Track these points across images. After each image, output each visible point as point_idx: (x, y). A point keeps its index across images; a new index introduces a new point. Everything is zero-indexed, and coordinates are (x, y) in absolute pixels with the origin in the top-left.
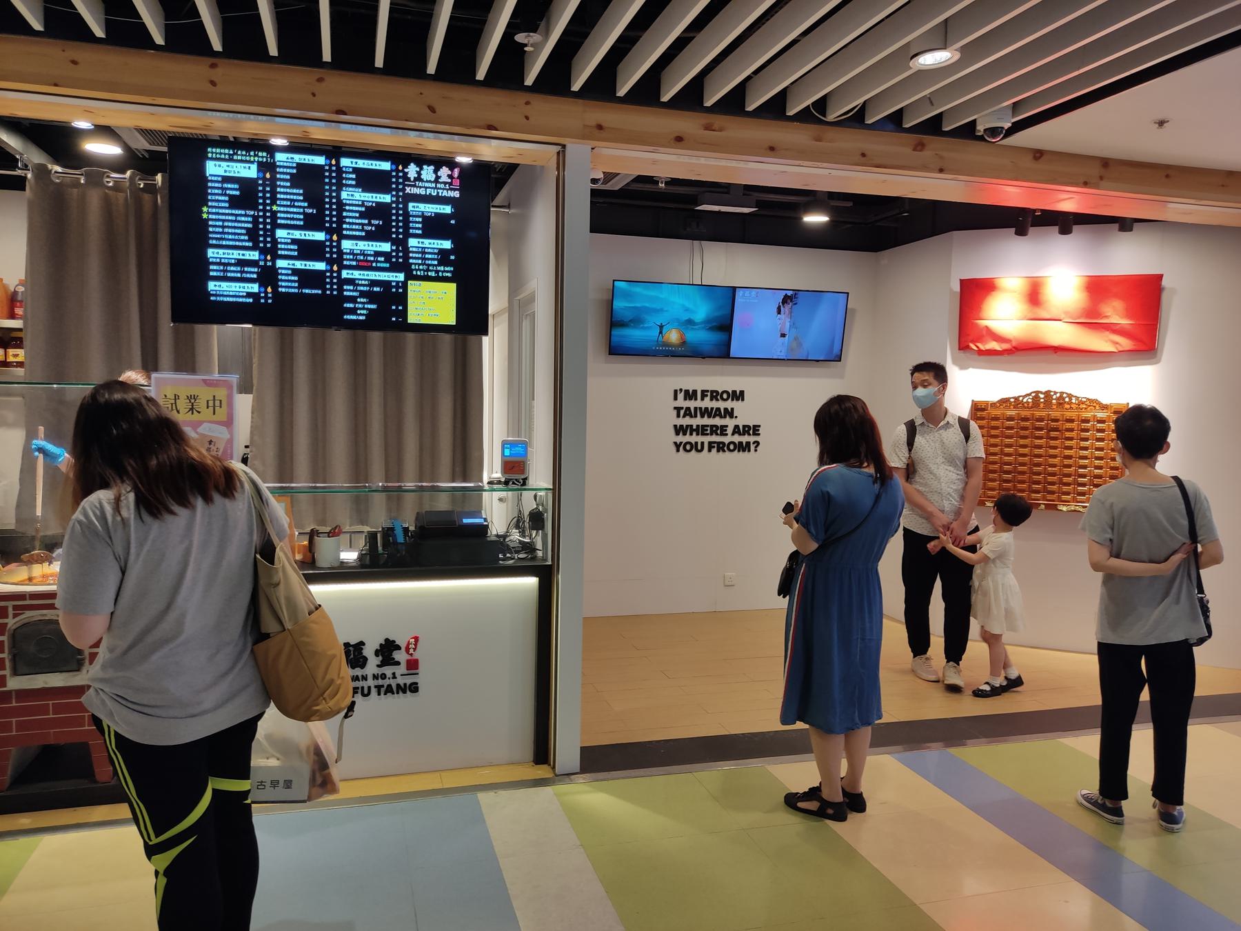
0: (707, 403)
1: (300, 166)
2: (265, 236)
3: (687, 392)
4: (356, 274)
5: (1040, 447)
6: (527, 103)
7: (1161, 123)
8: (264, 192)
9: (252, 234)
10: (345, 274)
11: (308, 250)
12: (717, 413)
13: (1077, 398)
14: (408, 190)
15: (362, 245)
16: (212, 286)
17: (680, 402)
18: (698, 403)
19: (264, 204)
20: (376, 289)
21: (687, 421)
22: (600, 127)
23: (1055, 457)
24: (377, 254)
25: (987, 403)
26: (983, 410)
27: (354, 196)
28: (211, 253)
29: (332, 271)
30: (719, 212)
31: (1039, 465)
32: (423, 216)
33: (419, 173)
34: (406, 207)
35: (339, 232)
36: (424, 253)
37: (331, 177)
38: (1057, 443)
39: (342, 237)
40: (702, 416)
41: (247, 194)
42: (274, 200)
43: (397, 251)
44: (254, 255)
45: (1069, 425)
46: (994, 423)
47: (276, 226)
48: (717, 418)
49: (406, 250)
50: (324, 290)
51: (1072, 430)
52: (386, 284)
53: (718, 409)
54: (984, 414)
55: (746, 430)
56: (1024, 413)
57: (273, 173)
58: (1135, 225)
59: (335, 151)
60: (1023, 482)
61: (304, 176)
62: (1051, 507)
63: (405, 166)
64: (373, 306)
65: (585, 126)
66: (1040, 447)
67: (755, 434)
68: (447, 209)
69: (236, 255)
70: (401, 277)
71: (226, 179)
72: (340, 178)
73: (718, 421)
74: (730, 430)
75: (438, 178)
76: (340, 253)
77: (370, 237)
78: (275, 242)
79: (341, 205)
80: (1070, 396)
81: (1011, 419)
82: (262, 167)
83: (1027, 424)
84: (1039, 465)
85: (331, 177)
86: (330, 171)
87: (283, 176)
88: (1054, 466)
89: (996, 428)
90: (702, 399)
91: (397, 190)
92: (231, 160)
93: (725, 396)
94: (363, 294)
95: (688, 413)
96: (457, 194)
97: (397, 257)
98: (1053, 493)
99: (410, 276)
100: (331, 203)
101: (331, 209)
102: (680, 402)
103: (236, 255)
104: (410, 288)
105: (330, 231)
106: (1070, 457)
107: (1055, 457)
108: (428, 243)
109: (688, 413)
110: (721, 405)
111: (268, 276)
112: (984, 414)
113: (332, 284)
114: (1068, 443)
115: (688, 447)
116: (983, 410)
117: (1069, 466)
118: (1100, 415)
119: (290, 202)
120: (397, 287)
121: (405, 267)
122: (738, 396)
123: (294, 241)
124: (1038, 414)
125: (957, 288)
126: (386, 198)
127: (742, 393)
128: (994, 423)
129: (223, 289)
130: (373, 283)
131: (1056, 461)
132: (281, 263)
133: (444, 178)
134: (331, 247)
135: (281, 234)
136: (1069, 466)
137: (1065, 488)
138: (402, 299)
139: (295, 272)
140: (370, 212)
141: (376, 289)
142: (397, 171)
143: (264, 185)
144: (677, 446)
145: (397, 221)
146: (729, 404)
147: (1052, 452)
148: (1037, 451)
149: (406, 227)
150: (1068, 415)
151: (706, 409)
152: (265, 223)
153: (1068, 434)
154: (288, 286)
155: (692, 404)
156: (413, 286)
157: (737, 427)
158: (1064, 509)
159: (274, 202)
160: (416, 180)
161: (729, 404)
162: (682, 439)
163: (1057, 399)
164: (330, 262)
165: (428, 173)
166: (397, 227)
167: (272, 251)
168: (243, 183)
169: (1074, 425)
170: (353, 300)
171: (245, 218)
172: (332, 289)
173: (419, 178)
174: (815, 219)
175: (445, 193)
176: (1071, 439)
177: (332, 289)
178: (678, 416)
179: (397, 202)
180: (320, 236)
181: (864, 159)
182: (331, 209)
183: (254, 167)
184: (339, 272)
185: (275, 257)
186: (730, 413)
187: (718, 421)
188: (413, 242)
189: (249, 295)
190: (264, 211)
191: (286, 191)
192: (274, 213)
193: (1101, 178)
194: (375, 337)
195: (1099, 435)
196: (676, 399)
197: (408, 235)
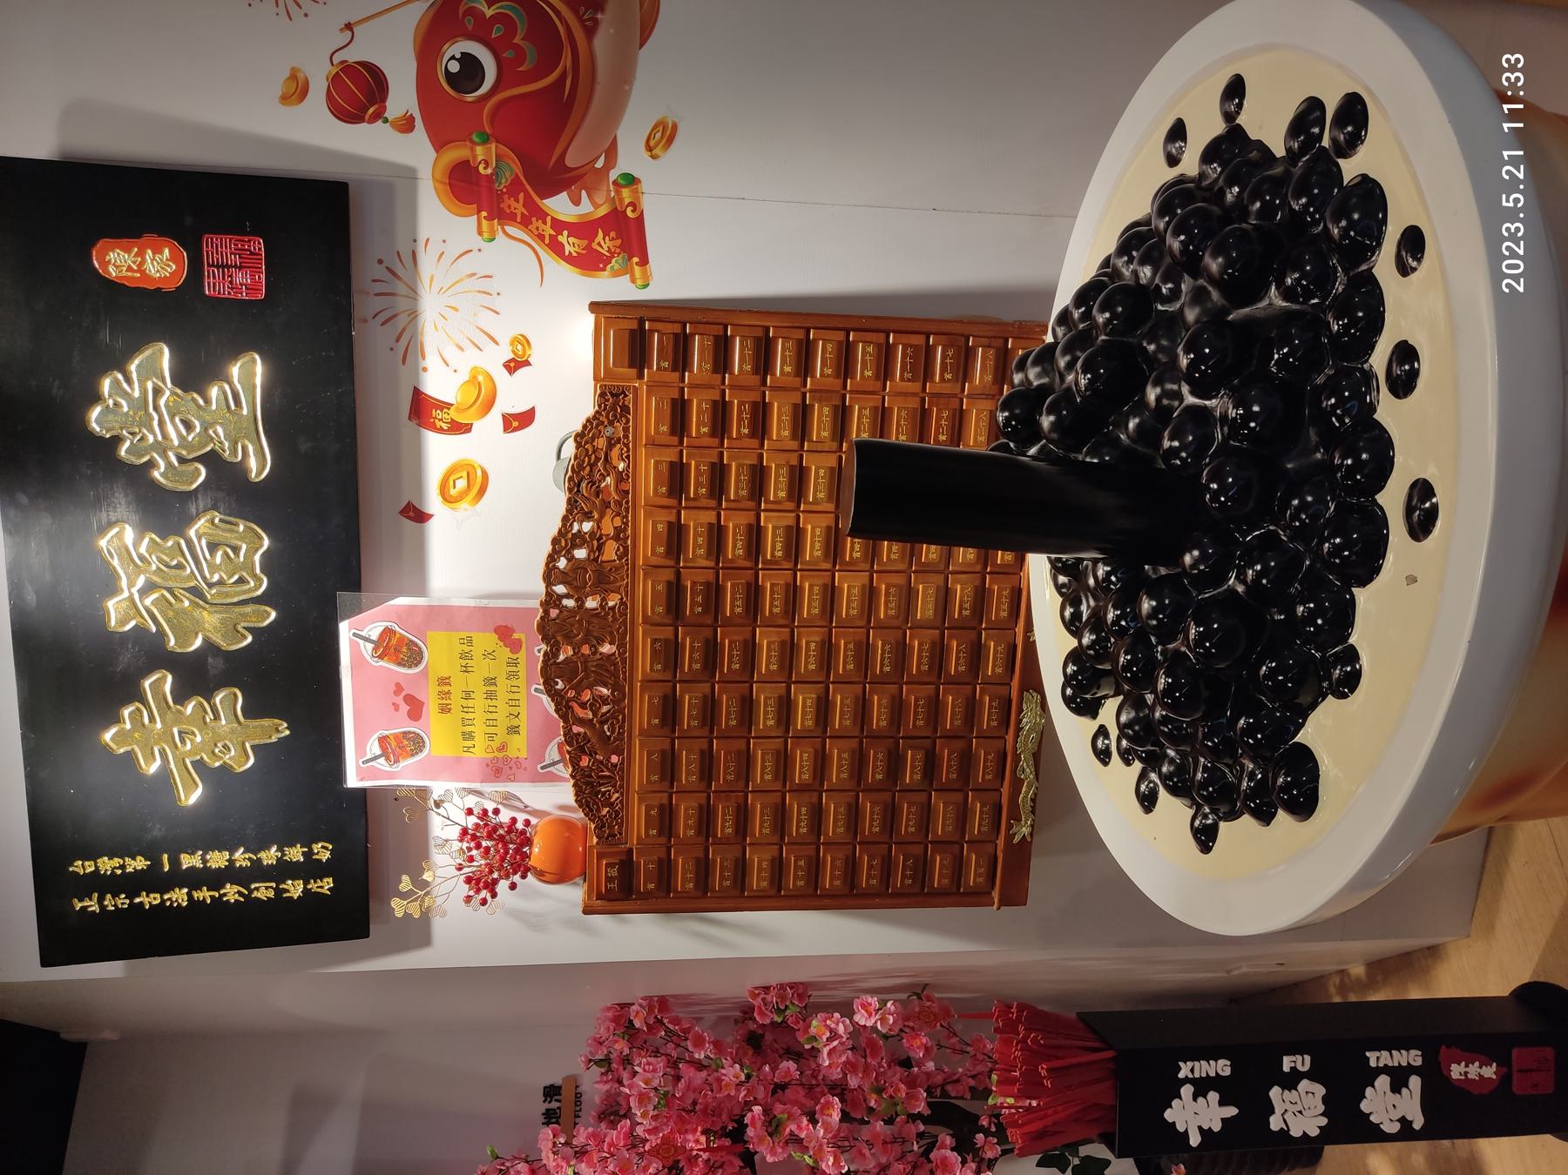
5: (789, 651)
23: (830, 595)
26: (627, 866)
31: (864, 653)
45: (696, 546)
46: (685, 825)
51: (717, 534)
54: (645, 865)
60: (935, 708)
66: (789, 651)
80: (564, 542)
81: (667, 766)
83: (690, 646)
84: (864, 653)
88: (871, 594)
89: (706, 820)
112: (645, 865)
114: (773, 546)
116: (627, 866)
118: (650, 414)
124: (644, 662)
128: (685, 825)
147: (810, 605)
148: (807, 662)
150: (647, 546)
153: (735, 548)
163: (579, 594)
169: (696, 523)
176: (755, 535)
195: (738, 427)
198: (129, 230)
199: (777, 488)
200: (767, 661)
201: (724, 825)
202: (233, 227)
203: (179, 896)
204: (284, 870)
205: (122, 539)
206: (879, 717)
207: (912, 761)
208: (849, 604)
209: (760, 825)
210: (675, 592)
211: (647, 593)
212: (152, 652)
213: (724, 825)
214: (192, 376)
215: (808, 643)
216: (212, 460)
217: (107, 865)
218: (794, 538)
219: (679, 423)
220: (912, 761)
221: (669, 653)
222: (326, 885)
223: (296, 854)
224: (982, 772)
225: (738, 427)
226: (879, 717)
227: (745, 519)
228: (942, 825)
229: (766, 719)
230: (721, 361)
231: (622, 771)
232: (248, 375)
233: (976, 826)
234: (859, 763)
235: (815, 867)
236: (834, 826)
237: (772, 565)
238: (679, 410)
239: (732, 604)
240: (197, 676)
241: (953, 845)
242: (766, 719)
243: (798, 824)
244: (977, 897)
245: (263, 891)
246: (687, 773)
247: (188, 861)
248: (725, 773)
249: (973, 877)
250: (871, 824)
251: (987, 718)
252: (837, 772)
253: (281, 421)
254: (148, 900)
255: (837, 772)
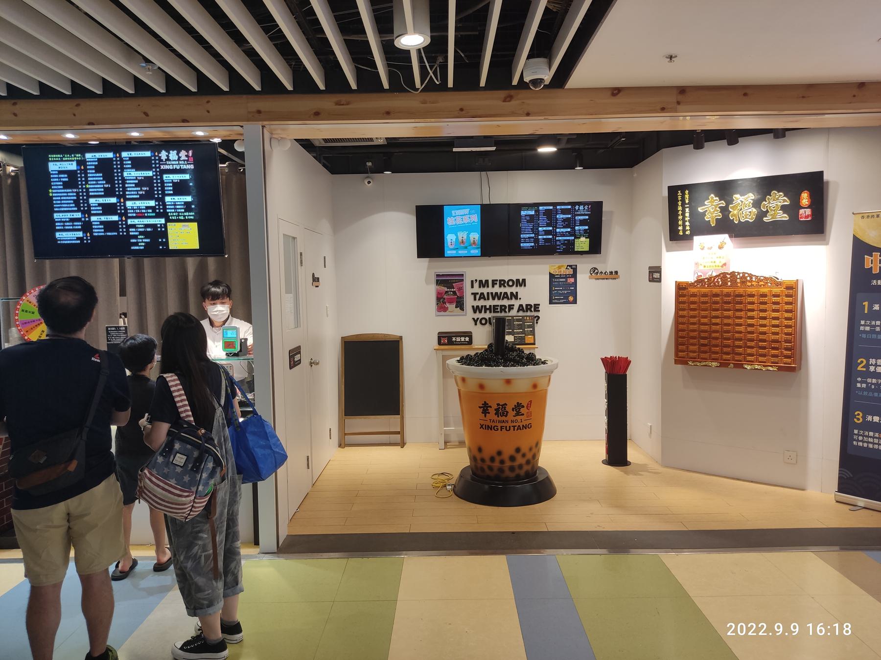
0: (497, 289)
1: (99, 160)
2: (83, 203)
3: (481, 281)
4: (136, 221)
5: (728, 317)
6: (208, 102)
7: (671, 57)
8: (81, 177)
9: (77, 202)
10: (130, 222)
11: (108, 209)
12: (505, 296)
13: (575, 284)
14: (162, 167)
15: (139, 204)
16: (58, 235)
17: (477, 289)
18: (490, 290)
19: (82, 185)
20: (149, 230)
21: (482, 303)
22: (259, 112)
23: (741, 325)
24: (147, 208)
25: (687, 283)
27: (131, 174)
28: (56, 216)
29: (122, 221)
30: (472, 152)
31: (728, 332)
32: (173, 182)
33: (168, 156)
34: (162, 178)
35: (124, 196)
36: (175, 205)
37: (117, 164)
38: (742, 314)
39: (126, 199)
40: (494, 299)
41: (72, 180)
42: (87, 182)
43: (159, 205)
44: (78, 215)
45: (750, 299)
46: (692, 299)
47: (89, 197)
48: (505, 300)
49: (164, 205)
50: (119, 232)
51: (753, 303)
52: (154, 226)
53: (505, 293)
54: (685, 292)
55: (529, 307)
56: (716, 290)
57: (85, 166)
58: (787, 133)
59: (117, 147)
60: (717, 346)
61: (104, 167)
62: (739, 366)
63: (159, 153)
64: (148, 240)
65: (249, 112)
66: (728, 317)
67: (535, 311)
68: (187, 177)
69: (69, 215)
70: (163, 221)
71: (60, 172)
72: (122, 164)
73: (506, 302)
74: (516, 308)
75: (179, 157)
76: (126, 209)
77: (142, 198)
78: (89, 206)
79: (124, 180)
80: (751, 276)
81: (705, 295)
82: (79, 163)
84: (728, 332)
85: (117, 164)
86: (116, 161)
87: (90, 166)
88: (740, 332)
89: (694, 303)
90: (493, 286)
91: (156, 168)
92: (62, 161)
93: (511, 283)
94: (141, 233)
95: (482, 296)
96: (192, 167)
97: (159, 209)
98: (740, 354)
99: (168, 220)
100: (118, 180)
101: (118, 184)
102: (477, 289)
103: (69, 215)
104: (169, 227)
105: (119, 197)
106: (752, 325)
107: (741, 325)
108: (177, 199)
109: (482, 296)
110: (508, 290)
111: (87, 227)
112: (685, 292)
113: (122, 228)
114: (750, 314)
115: (483, 322)
116: (685, 289)
117: (752, 333)
118: (776, 290)
119: (96, 182)
120: (161, 227)
121: (164, 215)
122: (522, 283)
123: (100, 205)
124: (726, 290)
125: (666, 193)
126: (150, 174)
127: (524, 280)
128: (692, 299)
129: (65, 237)
130: (147, 226)
131: (742, 329)
132: (93, 218)
133: (183, 158)
134: (120, 206)
135: (92, 201)
136: (752, 333)
137: (749, 351)
138: (165, 234)
139: (102, 223)
140: (140, 183)
141: (149, 230)
142: (155, 156)
143: (81, 173)
144: (475, 321)
145: (157, 187)
146: (514, 289)
147: (738, 321)
148: (726, 321)
149: (163, 190)
150: (749, 291)
151: (496, 293)
152: (83, 196)
153: (750, 307)
154: (99, 231)
155: (485, 291)
156: (170, 226)
157: (521, 306)
158: (749, 367)
159: (87, 183)
160: (166, 160)
161: (514, 289)
162: (478, 315)
163: (741, 278)
164: (120, 215)
165: (173, 155)
166: (158, 190)
167: (88, 212)
168: (70, 173)
169: (754, 299)
170: (135, 237)
171: (72, 193)
172: (123, 232)
173: (168, 159)
174: (547, 150)
175: (185, 167)
176: (753, 310)
177: (123, 232)
178: (475, 299)
179: (156, 175)
180: (113, 200)
181: (462, 113)
182: (118, 184)
183: (75, 163)
184: (126, 221)
185: (90, 215)
186: (515, 296)
187: (506, 302)
188: (168, 199)
189: (78, 238)
190: (82, 188)
191: (91, 174)
192: (87, 189)
193: (678, 103)
194: (147, 262)
195: (774, 307)
196: (472, 287)
197: (164, 195)
198: (812, 197)
199: (762, 314)
200: (726, 313)
201: (692, 306)
202: (813, 214)
203: (680, 208)
204: (684, 226)
205: (751, 197)
206: (714, 335)
207: (706, 342)
208: (738, 328)
209: (692, 313)
210: (741, 296)
211: (741, 291)
212: (729, 202)
213: (692, 306)
214: (784, 208)
215: (729, 321)
216: (767, 211)
217: (687, 196)
218: (752, 318)
219: (775, 296)
220: (706, 342)
221: (728, 295)
222: (681, 233)
223: (688, 228)
224: (703, 355)
225: (774, 307)
226: (714, 335)
227: (756, 308)
228: (691, 348)
229: (714, 313)
230: (787, 303)
231: (704, 287)
232: (785, 217)
233: (691, 354)
234: (705, 331)
235: (683, 324)
236: (692, 327)
237: (746, 314)
238: (778, 296)
239: (738, 307)
240: (724, 210)
241: (687, 350)
242: (714, 313)
243: (692, 320)
244: (676, 355)
245: (680, 223)
246: (703, 299)
247: (687, 210)
248: (703, 306)
249: (681, 354)
250: (692, 334)
251: (714, 356)
252: (703, 328)
253: (775, 223)
254: (680, 203)
255: (703, 328)
